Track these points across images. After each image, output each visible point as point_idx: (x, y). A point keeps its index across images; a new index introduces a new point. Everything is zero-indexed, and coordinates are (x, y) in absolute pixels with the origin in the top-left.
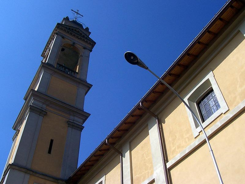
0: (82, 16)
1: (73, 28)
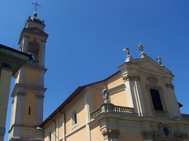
0: (40, 6)
1: (33, 28)
